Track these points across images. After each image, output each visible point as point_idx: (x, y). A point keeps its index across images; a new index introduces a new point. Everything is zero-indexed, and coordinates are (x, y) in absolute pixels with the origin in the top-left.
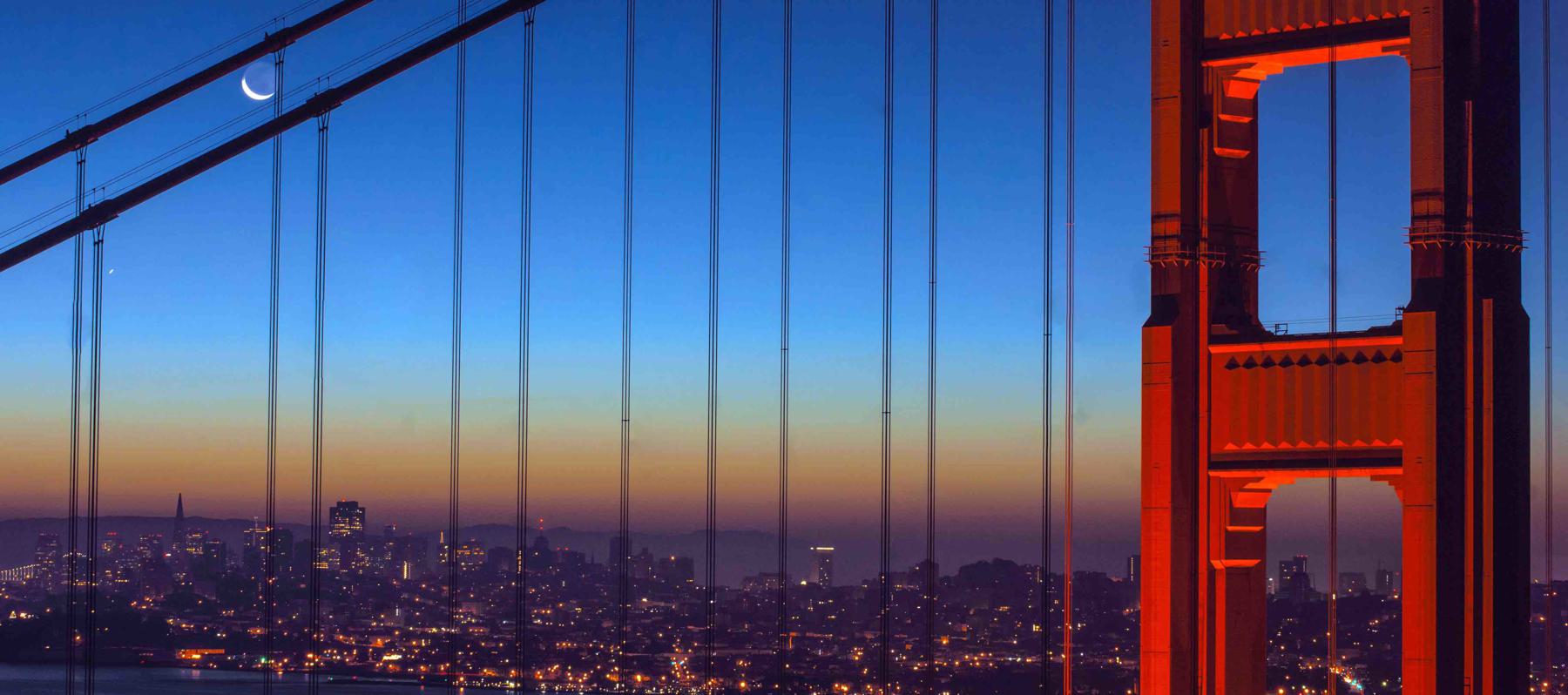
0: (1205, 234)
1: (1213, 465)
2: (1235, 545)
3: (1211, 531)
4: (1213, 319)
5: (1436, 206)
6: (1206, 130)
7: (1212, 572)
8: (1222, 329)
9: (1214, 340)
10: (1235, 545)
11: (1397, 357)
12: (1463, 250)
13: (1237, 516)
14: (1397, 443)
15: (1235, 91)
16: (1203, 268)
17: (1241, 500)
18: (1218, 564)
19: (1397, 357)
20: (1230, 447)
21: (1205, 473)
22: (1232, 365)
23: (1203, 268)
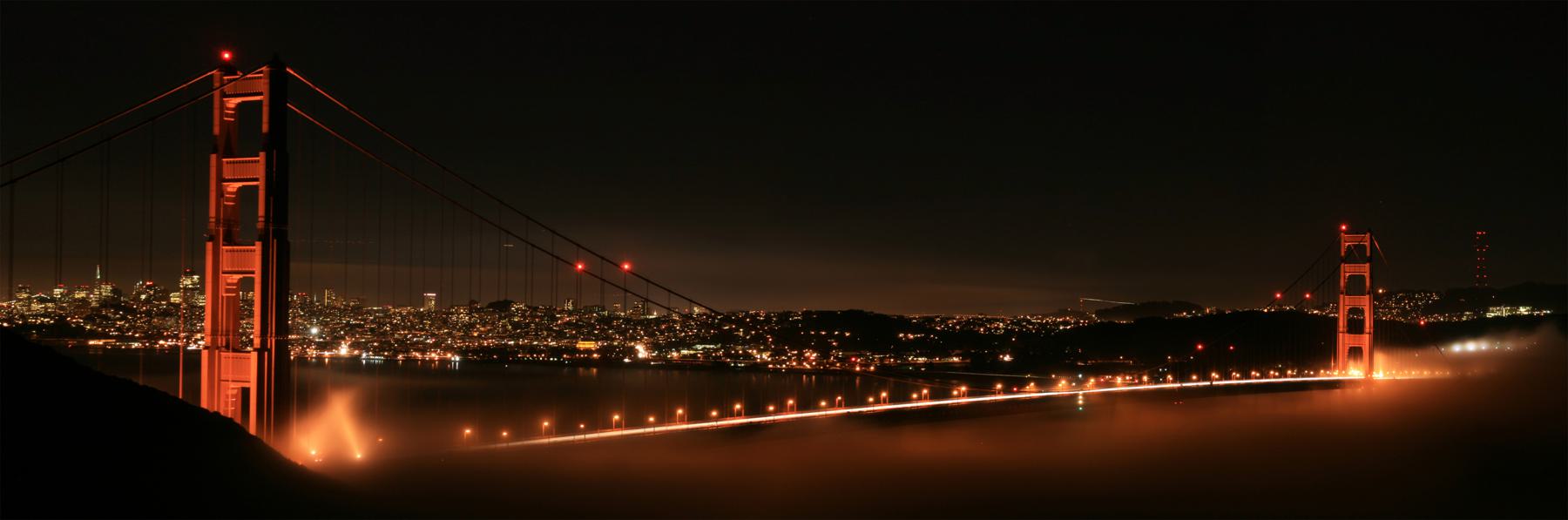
0: (222, 221)
1: (223, 273)
2: (228, 291)
3: (222, 287)
4: (224, 240)
5: (263, 219)
6: (222, 199)
7: (222, 297)
8: (225, 243)
9: (224, 245)
10: (228, 291)
11: (254, 251)
12: (269, 229)
13: (229, 284)
15: (229, 190)
16: (221, 230)
17: (229, 281)
18: (224, 295)
19: (254, 251)
20: (226, 269)
21: (221, 275)
22: (227, 251)
23: (221, 230)
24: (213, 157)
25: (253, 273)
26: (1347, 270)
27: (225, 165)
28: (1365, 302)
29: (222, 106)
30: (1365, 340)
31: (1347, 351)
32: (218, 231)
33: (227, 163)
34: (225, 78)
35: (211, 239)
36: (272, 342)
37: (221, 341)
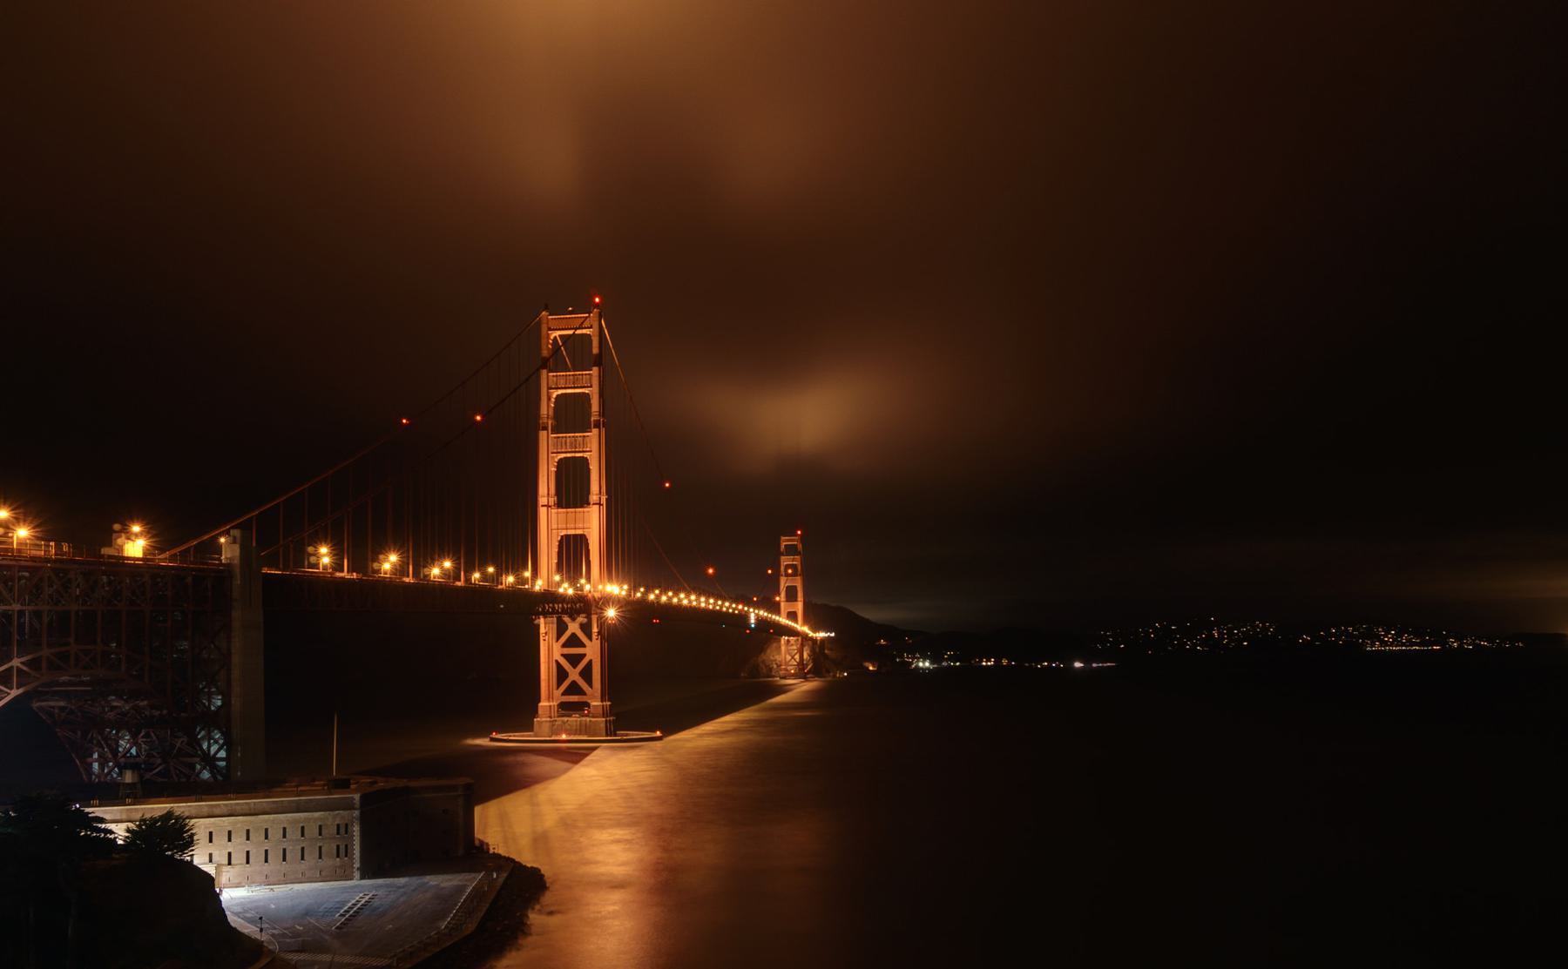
4: (552, 430)
14: (588, 449)
16: (550, 422)
21: (551, 455)
24: (544, 372)
25: (591, 451)
26: (785, 561)
27: (550, 378)
28: (798, 583)
29: (548, 335)
30: (799, 607)
31: (786, 612)
32: (548, 423)
33: (553, 376)
34: (550, 317)
35: (545, 428)
36: (604, 501)
37: (552, 500)
